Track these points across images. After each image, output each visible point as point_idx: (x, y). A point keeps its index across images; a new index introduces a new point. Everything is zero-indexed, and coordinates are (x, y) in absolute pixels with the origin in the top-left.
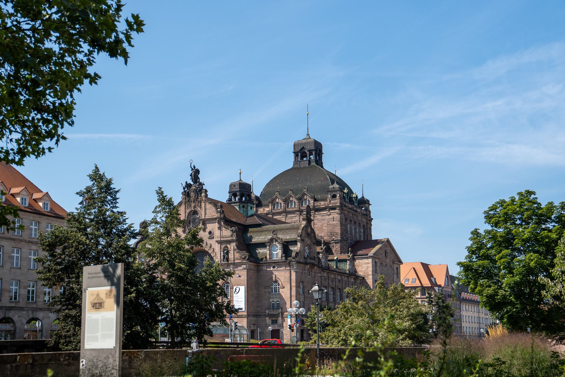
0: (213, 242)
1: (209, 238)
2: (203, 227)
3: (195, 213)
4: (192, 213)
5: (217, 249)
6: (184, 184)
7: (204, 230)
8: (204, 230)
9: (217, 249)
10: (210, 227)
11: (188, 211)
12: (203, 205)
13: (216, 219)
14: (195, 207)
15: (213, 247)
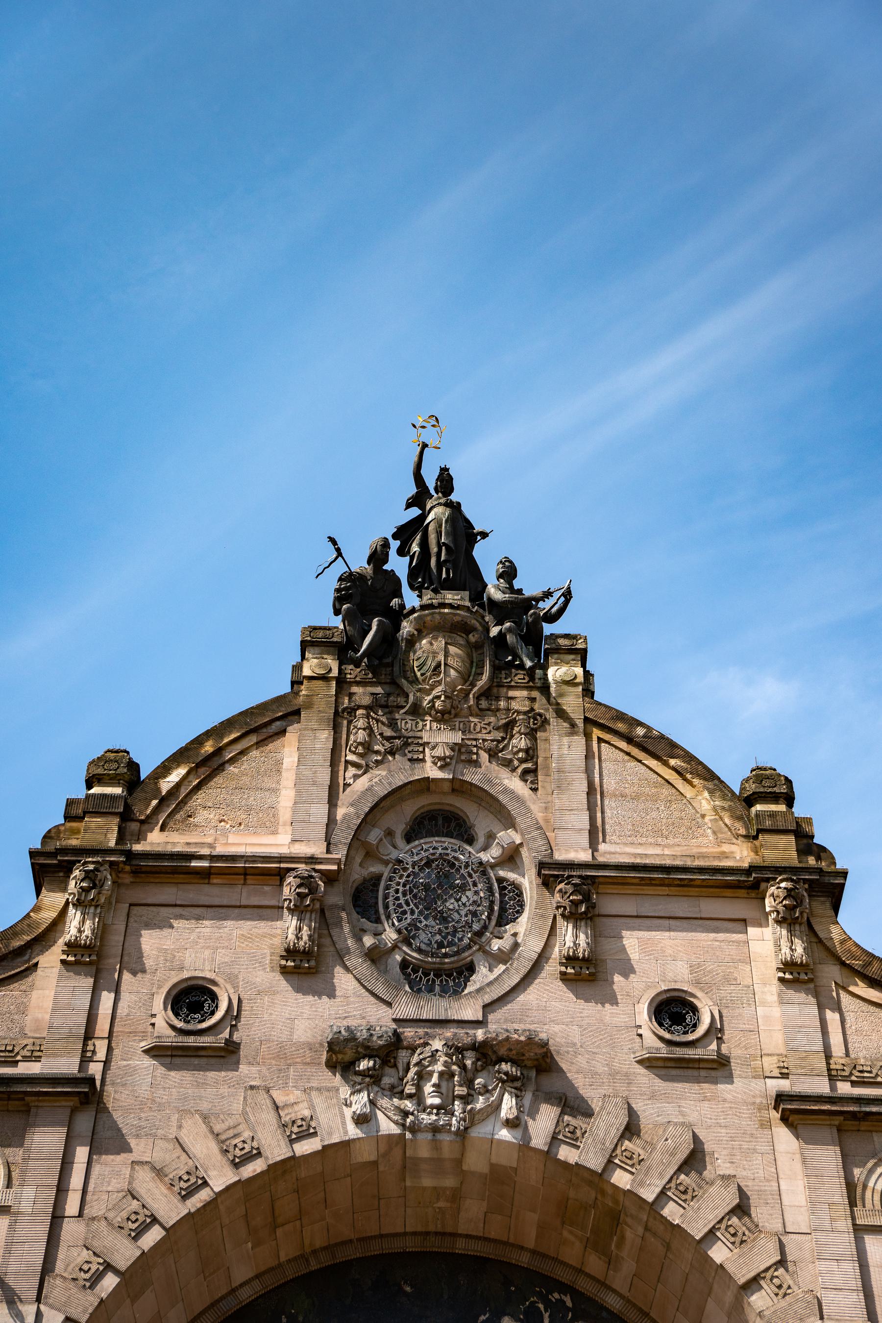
0: (727, 1117)
1: (673, 1066)
2: (571, 938)
3: (444, 814)
4: (399, 820)
5: (795, 1192)
6: (358, 561)
7: (588, 974)
8: (588, 974)
9: (795, 1192)
10: (658, 955)
11: (364, 786)
12: (563, 749)
13: (749, 883)
14: (462, 755)
15: (720, 1163)
